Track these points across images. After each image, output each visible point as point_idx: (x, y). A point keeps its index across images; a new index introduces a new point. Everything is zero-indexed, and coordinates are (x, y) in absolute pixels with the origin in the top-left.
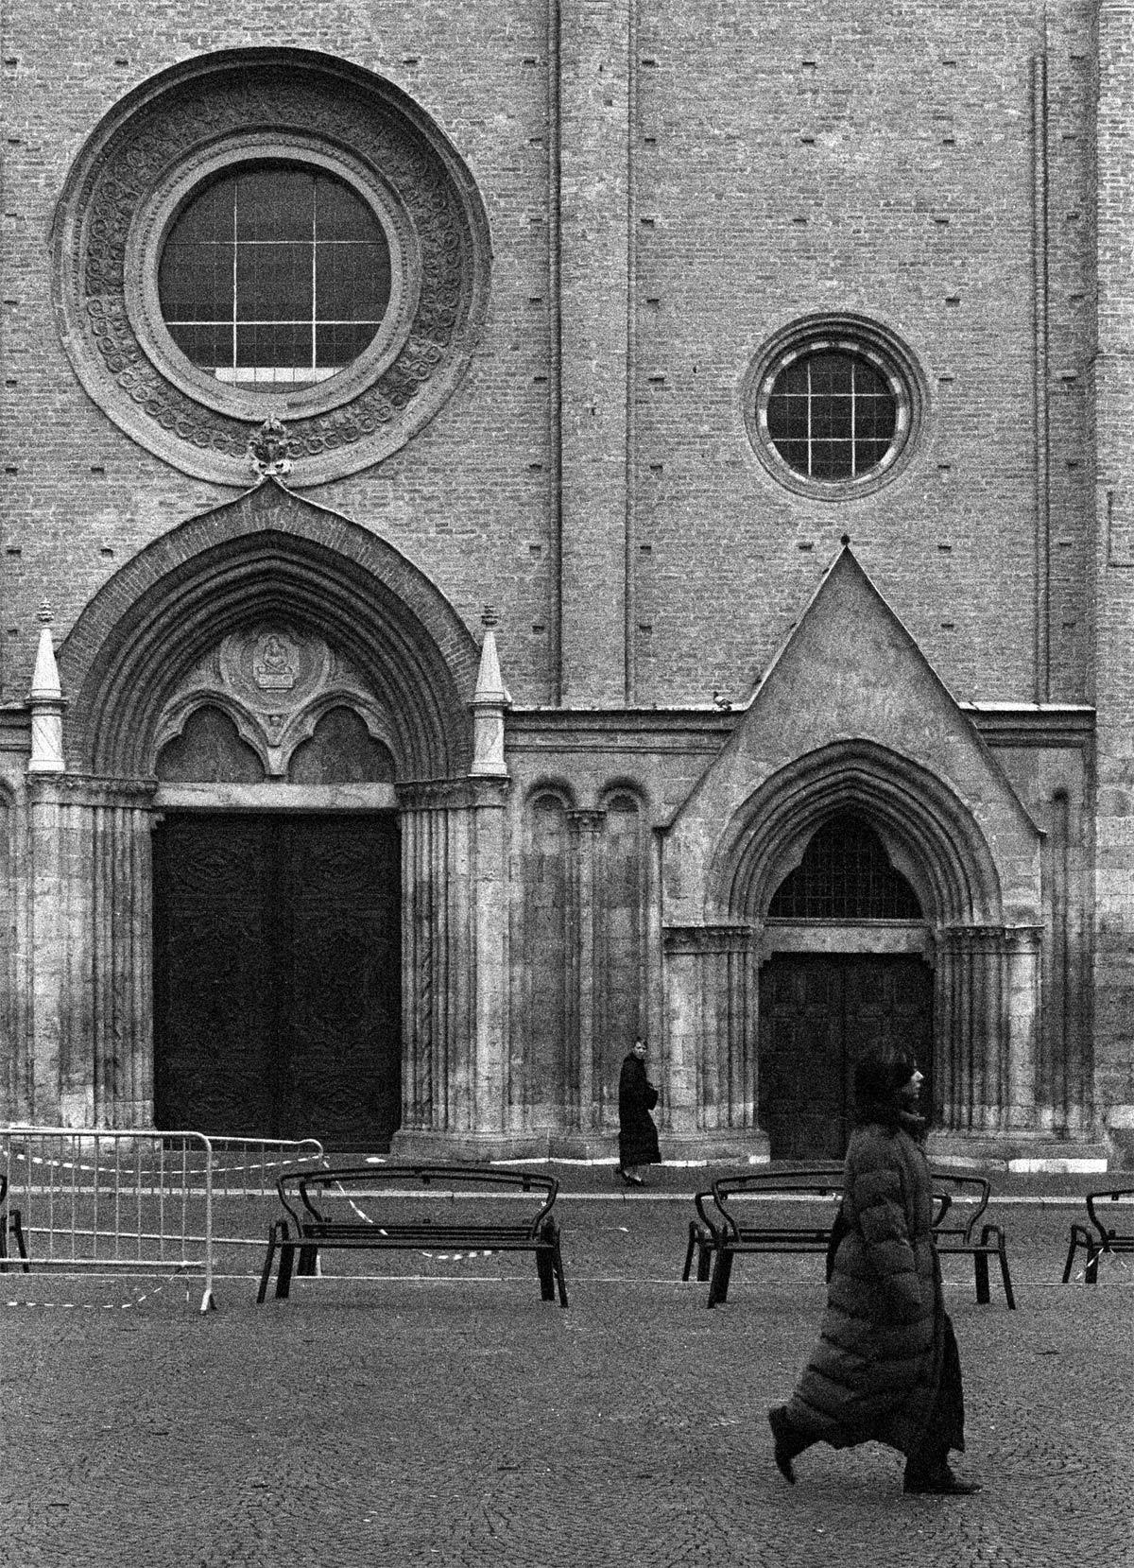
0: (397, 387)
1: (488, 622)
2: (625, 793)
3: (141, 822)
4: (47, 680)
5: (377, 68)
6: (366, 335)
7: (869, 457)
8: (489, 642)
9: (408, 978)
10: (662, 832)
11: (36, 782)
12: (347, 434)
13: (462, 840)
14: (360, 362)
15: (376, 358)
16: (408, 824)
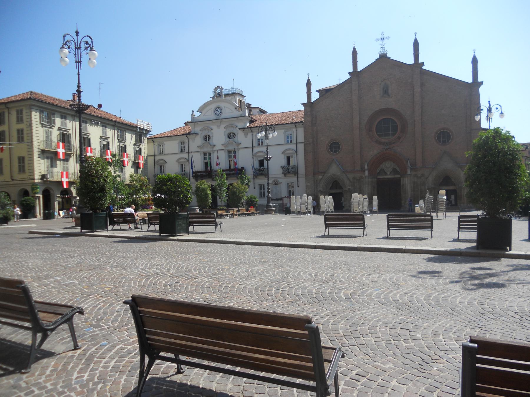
0: (399, 138)
1: (408, 159)
2: (423, 175)
3: (376, 180)
4: (366, 167)
5: (396, 109)
6: (396, 133)
7: (448, 141)
8: (409, 161)
9: (402, 193)
10: (427, 178)
11: (366, 177)
12: (394, 143)
13: (406, 180)
14: (395, 136)
15: (396, 135)
16: (401, 179)
